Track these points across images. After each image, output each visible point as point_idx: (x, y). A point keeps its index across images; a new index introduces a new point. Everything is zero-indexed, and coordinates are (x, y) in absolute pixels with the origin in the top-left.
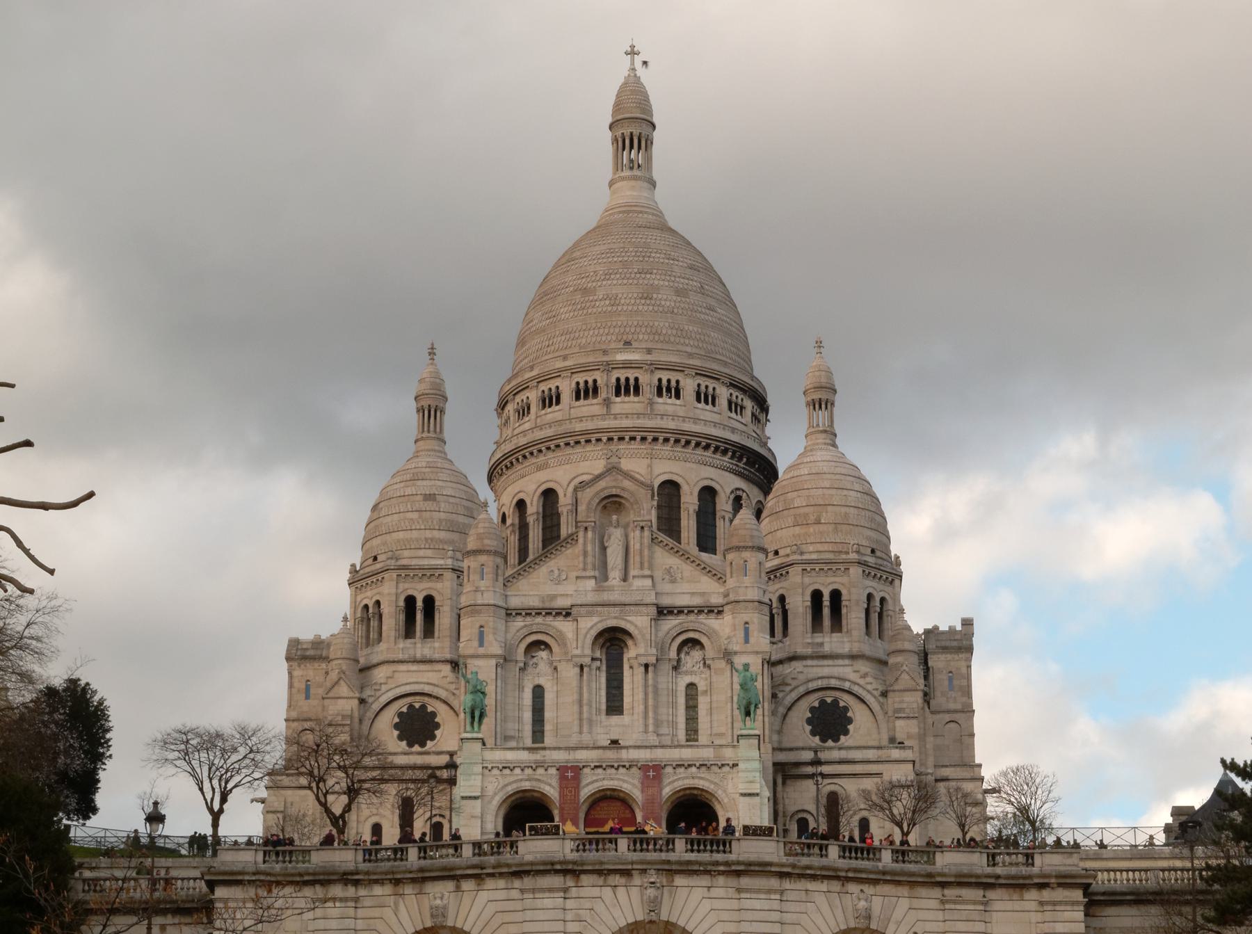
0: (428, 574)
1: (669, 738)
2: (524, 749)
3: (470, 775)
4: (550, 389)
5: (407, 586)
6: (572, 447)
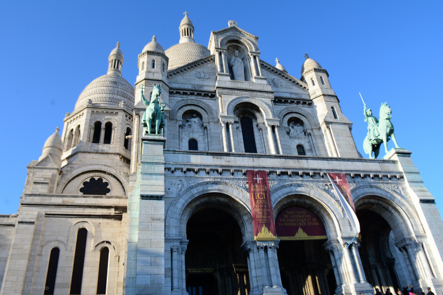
0: (110, 112)
2: (208, 154)
3: (151, 174)
5: (97, 116)
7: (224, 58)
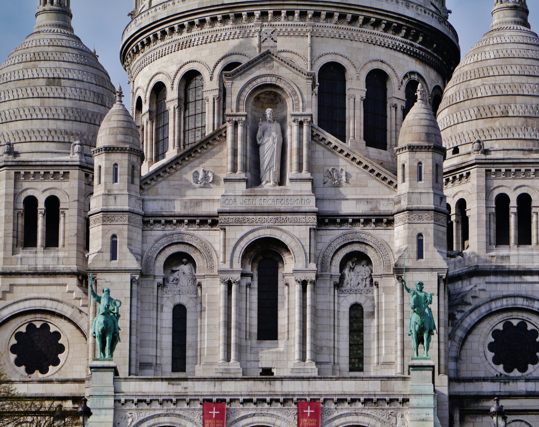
0: (52, 172)
1: (330, 366)
2: (162, 380)
3: (100, 409)
5: (26, 185)
6: (221, 22)
7: (242, 137)
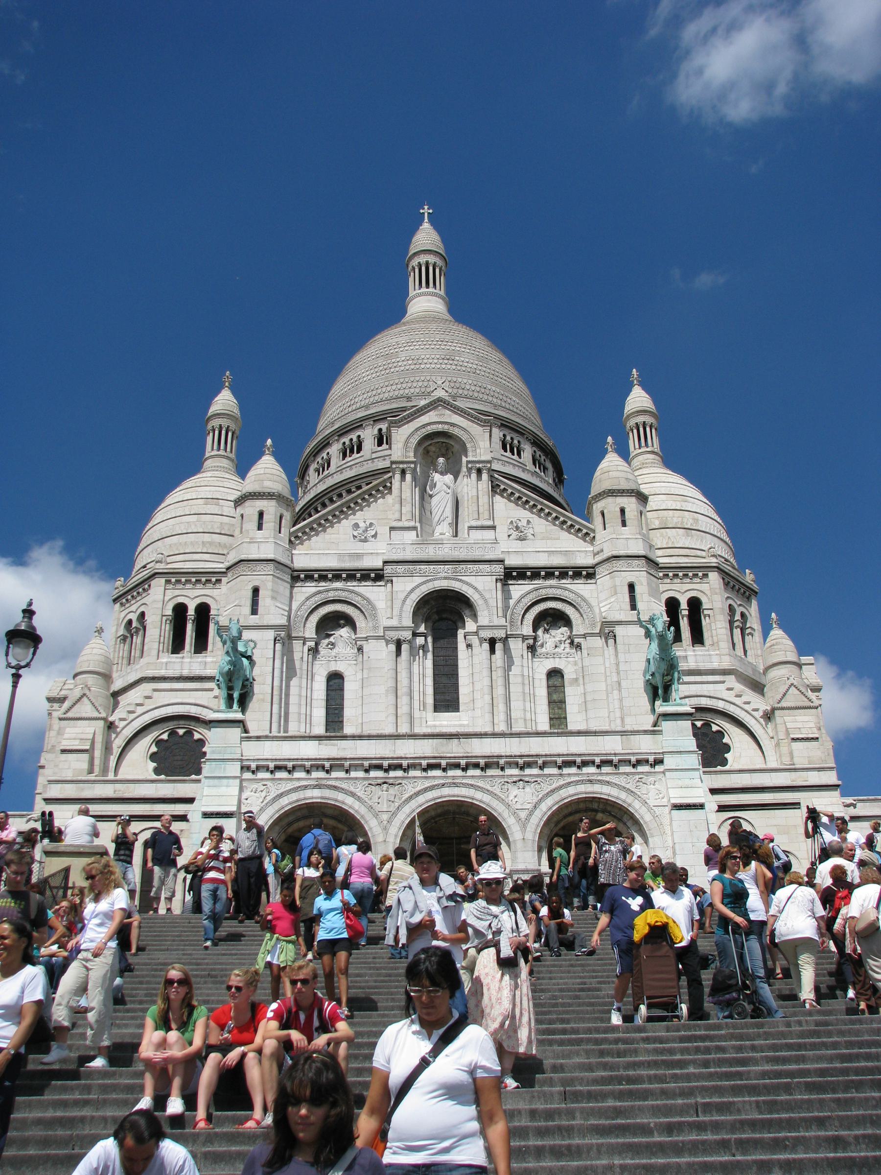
0: (203, 579)
4: (351, 440)
5: (177, 592)
